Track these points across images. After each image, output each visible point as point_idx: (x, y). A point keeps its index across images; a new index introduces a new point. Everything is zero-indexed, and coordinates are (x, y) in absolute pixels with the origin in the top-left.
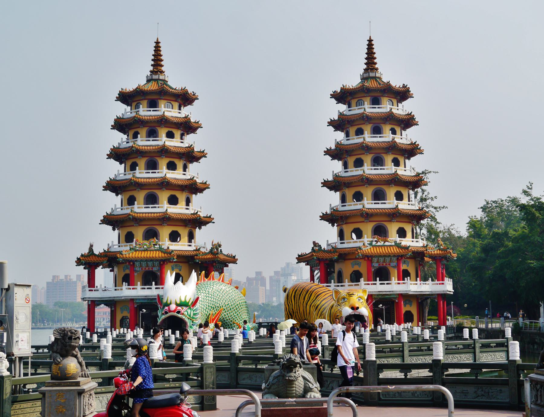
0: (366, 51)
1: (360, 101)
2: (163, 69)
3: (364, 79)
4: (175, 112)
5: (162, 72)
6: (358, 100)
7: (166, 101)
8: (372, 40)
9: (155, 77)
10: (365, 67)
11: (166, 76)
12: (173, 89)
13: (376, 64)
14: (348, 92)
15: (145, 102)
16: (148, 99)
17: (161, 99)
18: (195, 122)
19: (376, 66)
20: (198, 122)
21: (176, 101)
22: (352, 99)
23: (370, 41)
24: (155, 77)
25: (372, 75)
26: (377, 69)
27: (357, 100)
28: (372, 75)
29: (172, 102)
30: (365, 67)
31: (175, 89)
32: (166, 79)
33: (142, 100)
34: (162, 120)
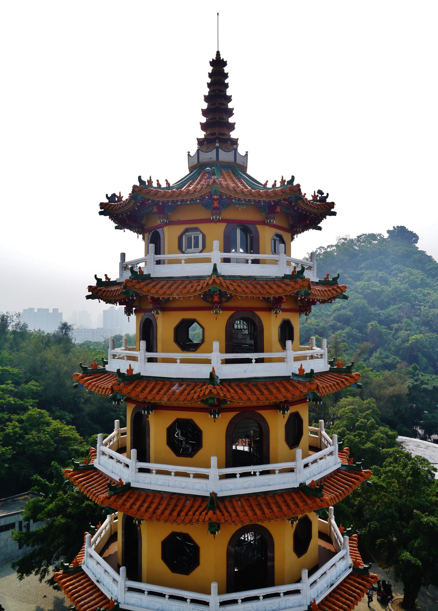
0: (206, 91)
1: (193, 235)
3: (197, 167)
6: (187, 230)
8: (224, 64)
10: (202, 134)
13: (232, 127)
14: (156, 204)
19: (233, 135)
22: (166, 224)
23: (218, 64)
25: (225, 156)
26: (235, 142)
27: (181, 228)
28: (225, 156)
30: (202, 134)
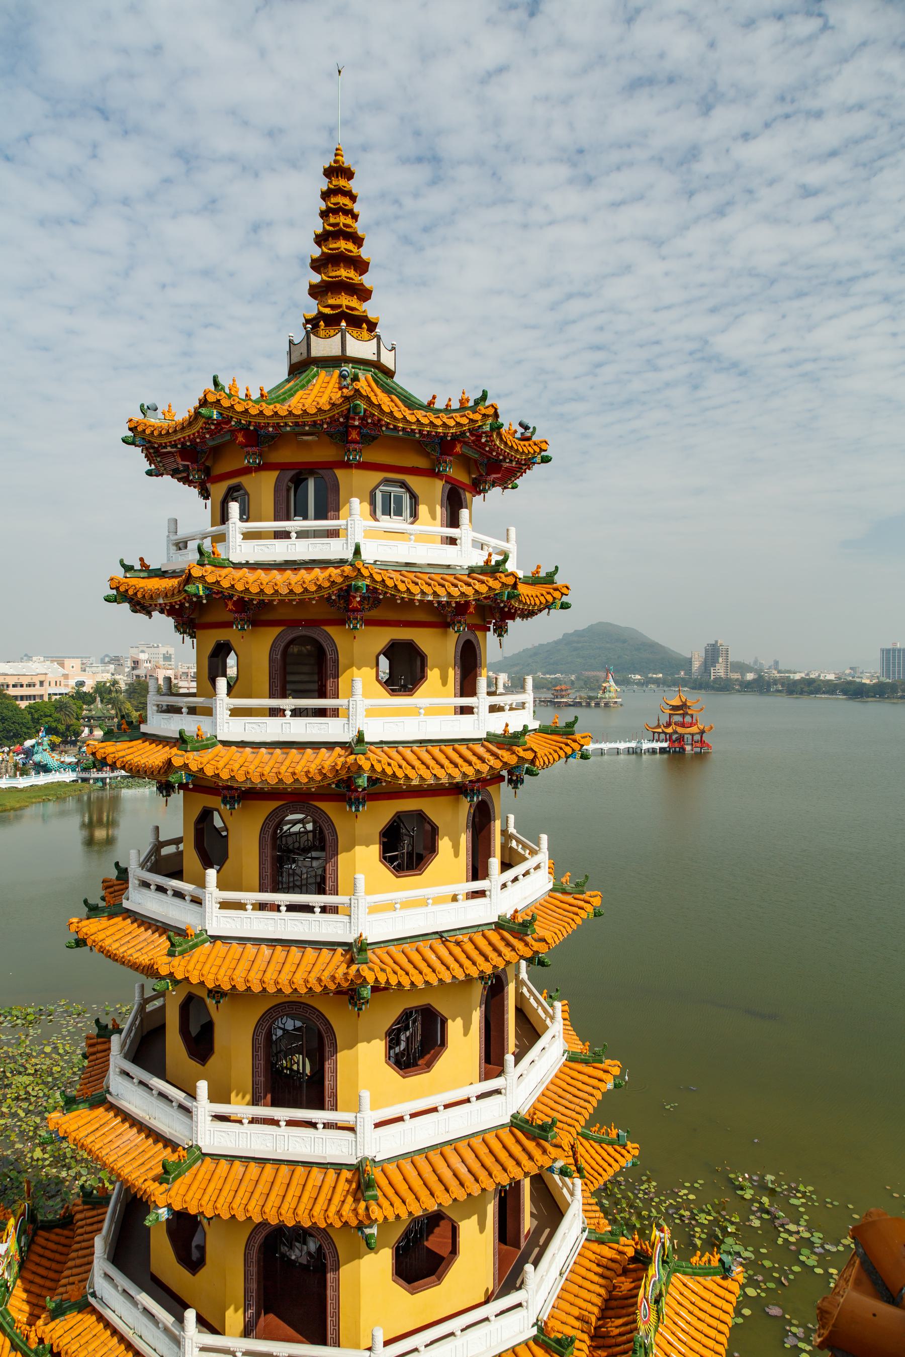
2: (370, 309)
4: (424, 538)
5: (364, 324)
7: (377, 477)
9: (325, 346)
11: (386, 341)
12: (410, 403)
15: (264, 487)
16: (281, 467)
17: (347, 465)
18: (534, 581)
20: (549, 579)
21: (431, 473)
24: (325, 346)
29: (413, 481)
31: (429, 407)
32: (387, 359)
33: (246, 471)
34: (346, 592)
